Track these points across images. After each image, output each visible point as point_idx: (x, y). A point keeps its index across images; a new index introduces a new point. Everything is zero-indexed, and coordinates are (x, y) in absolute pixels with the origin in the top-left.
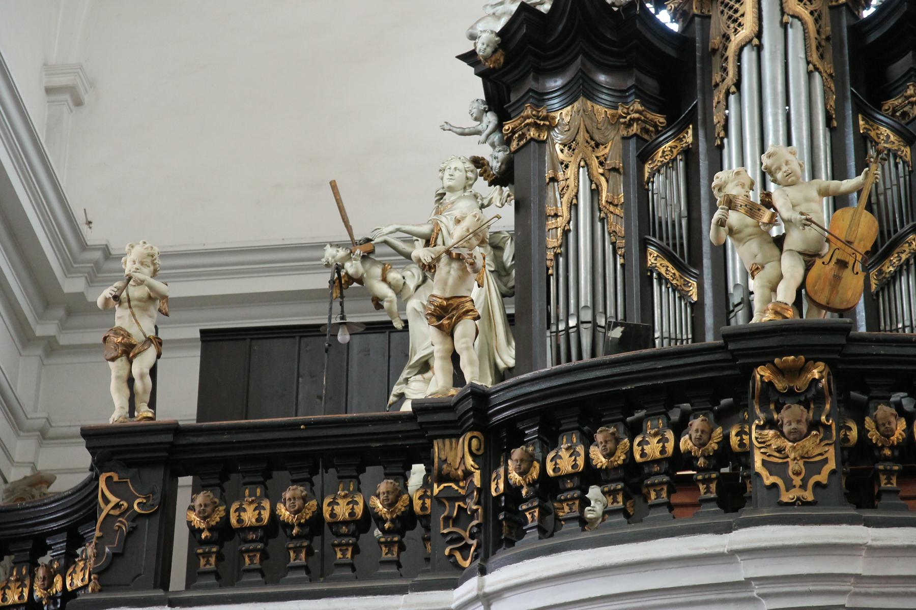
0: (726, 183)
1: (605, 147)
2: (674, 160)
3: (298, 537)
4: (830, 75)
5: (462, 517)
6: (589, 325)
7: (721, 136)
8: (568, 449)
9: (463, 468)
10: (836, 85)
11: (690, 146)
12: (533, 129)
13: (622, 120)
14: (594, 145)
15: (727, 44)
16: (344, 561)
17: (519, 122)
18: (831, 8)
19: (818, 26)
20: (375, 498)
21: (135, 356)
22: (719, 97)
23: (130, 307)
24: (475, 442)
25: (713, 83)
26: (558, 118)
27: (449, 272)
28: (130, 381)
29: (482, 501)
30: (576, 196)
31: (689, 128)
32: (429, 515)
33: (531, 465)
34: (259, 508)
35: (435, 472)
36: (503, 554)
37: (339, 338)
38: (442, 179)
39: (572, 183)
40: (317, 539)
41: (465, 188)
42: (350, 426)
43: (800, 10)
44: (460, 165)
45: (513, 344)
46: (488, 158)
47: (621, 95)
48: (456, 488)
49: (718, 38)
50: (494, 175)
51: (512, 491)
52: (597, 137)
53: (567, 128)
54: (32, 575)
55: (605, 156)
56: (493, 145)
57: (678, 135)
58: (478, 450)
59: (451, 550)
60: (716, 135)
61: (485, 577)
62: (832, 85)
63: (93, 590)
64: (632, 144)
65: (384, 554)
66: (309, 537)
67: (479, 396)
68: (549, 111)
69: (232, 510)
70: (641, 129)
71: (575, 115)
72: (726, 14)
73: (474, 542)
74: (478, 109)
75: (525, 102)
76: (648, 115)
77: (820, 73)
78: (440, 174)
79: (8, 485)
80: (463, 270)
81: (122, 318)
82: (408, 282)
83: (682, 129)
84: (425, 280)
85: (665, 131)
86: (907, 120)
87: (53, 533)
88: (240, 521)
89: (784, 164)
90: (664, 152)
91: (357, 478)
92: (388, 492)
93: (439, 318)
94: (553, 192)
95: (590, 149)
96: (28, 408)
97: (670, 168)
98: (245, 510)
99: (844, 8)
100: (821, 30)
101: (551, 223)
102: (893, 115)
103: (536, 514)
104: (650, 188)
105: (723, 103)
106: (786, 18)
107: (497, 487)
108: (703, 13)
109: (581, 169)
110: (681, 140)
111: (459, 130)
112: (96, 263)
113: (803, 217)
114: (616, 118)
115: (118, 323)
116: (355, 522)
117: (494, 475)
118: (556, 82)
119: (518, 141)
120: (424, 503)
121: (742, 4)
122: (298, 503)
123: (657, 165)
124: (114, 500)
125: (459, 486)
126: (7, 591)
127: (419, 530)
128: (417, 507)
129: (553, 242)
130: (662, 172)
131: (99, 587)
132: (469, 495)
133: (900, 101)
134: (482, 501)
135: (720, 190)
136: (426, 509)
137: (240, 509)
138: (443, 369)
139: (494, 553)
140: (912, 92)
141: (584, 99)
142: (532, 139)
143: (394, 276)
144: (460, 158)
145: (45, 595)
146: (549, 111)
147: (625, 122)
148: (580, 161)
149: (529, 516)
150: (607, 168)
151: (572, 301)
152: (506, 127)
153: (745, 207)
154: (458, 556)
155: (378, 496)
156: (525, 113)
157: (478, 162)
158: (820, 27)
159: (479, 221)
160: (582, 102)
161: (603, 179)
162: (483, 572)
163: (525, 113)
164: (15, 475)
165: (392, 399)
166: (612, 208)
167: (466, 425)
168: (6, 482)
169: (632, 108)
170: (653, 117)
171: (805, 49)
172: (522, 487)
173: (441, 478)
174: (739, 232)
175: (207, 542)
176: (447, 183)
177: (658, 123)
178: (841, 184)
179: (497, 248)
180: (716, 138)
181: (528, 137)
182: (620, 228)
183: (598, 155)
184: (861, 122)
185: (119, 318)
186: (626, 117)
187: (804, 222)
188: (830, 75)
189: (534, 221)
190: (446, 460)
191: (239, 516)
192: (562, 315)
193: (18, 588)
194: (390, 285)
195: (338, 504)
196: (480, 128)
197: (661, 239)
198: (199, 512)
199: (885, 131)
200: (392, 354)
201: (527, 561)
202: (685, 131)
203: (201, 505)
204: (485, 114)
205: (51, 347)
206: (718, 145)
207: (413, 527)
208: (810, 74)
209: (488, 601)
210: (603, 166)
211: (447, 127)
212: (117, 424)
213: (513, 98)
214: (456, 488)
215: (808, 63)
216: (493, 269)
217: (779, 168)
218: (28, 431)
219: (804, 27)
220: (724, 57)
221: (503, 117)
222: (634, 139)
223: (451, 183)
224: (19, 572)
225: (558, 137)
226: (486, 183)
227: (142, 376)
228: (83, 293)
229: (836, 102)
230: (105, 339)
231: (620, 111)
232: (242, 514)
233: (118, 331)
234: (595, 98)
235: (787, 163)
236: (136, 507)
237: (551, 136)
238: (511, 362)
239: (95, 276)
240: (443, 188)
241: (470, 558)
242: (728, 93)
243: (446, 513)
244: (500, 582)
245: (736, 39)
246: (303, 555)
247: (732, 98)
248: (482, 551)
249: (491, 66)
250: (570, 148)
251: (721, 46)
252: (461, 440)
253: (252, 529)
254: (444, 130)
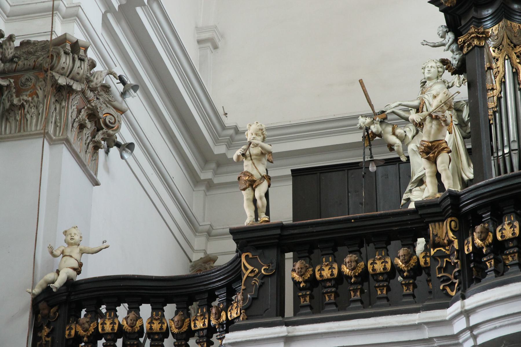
3: (355, 283)
5: (449, 267)
6: (517, 152)
8: (509, 224)
9: (447, 239)
12: (476, 40)
14: (513, 46)
16: (382, 296)
17: (467, 36)
20: (397, 259)
21: (256, 187)
23: (252, 159)
24: (453, 224)
26: (491, 32)
27: (431, 126)
28: (255, 201)
29: (460, 257)
30: (504, 77)
32: (429, 267)
33: (487, 235)
34: (331, 268)
35: (431, 242)
36: (474, 287)
37: (370, 169)
38: (424, 73)
39: (501, 69)
40: (366, 284)
41: (437, 78)
42: (380, 219)
44: (434, 64)
45: (472, 165)
46: (450, 59)
48: (444, 250)
50: (454, 68)
51: (477, 250)
52: (514, 41)
53: (496, 38)
54: (209, 312)
56: (453, 51)
58: (455, 228)
59: (444, 286)
61: (465, 301)
63: (243, 319)
65: (405, 290)
66: (361, 283)
67: (454, 196)
68: (485, 29)
69: (316, 270)
71: (501, 30)
73: (457, 281)
74: (443, 31)
75: (471, 25)
78: (423, 71)
79: (192, 263)
80: (440, 125)
81: (247, 166)
82: (408, 134)
84: (417, 132)
87: (219, 288)
88: (321, 276)
91: (386, 248)
92: (404, 255)
93: (427, 153)
94: (490, 76)
95: (511, 48)
96: (200, 219)
98: (323, 270)
101: (490, 94)
103: (493, 263)
107: (468, 249)
109: (506, 61)
111: (432, 44)
112: (231, 136)
115: (245, 169)
116: (387, 273)
117: (466, 242)
118: (488, 11)
119: (468, 48)
120: (426, 260)
122: (353, 264)
124: (250, 268)
125: (446, 249)
126: (196, 321)
127: (424, 275)
128: (422, 262)
129: (491, 104)
131: (246, 317)
132: (452, 254)
134: (460, 257)
136: (428, 263)
137: (321, 269)
138: (432, 183)
139: (469, 287)
141: (506, 20)
142: (476, 46)
143: (399, 131)
144: (433, 61)
145: (217, 323)
146: (485, 29)
148: (505, 56)
149: (488, 264)
151: (505, 138)
152: (460, 40)
154: (448, 289)
155: (399, 258)
156: (471, 31)
157: (444, 62)
159: (447, 96)
160: (505, 22)
162: (464, 298)
163: (471, 31)
164: (196, 257)
165: (403, 202)
167: (447, 214)
168: (191, 261)
172: (483, 248)
173: (435, 246)
175: (303, 289)
176: (427, 75)
179: (459, 111)
181: (473, 45)
183: (516, 51)
185: (246, 166)
189: (479, 94)
190: (437, 235)
191: (321, 273)
192: (500, 147)
193: (202, 320)
194: (397, 137)
195: (376, 263)
196: (444, 42)
198: (298, 272)
200: (401, 176)
201: (489, 291)
203: (299, 268)
204: (447, 34)
205: (210, 185)
207: (420, 274)
209: (468, 314)
210: (519, 58)
211: (425, 43)
212: (249, 225)
213: (463, 23)
214: (444, 250)
216: (457, 123)
218: (201, 233)
221: (457, 34)
223: (429, 75)
224: (202, 311)
225: (491, 43)
226: (450, 73)
227: (261, 198)
228: (225, 153)
230: (239, 178)
232: (322, 272)
233: (246, 173)
234: (512, 18)
236: (263, 271)
237: (487, 43)
238: (472, 176)
239: (231, 144)
240: (425, 78)
241: (455, 290)
243: (439, 265)
244: (474, 303)
246: (358, 293)
248: (462, 286)
249: (449, 5)
250: (499, 49)
252: (445, 223)
253: (328, 280)
254: (423, 45)
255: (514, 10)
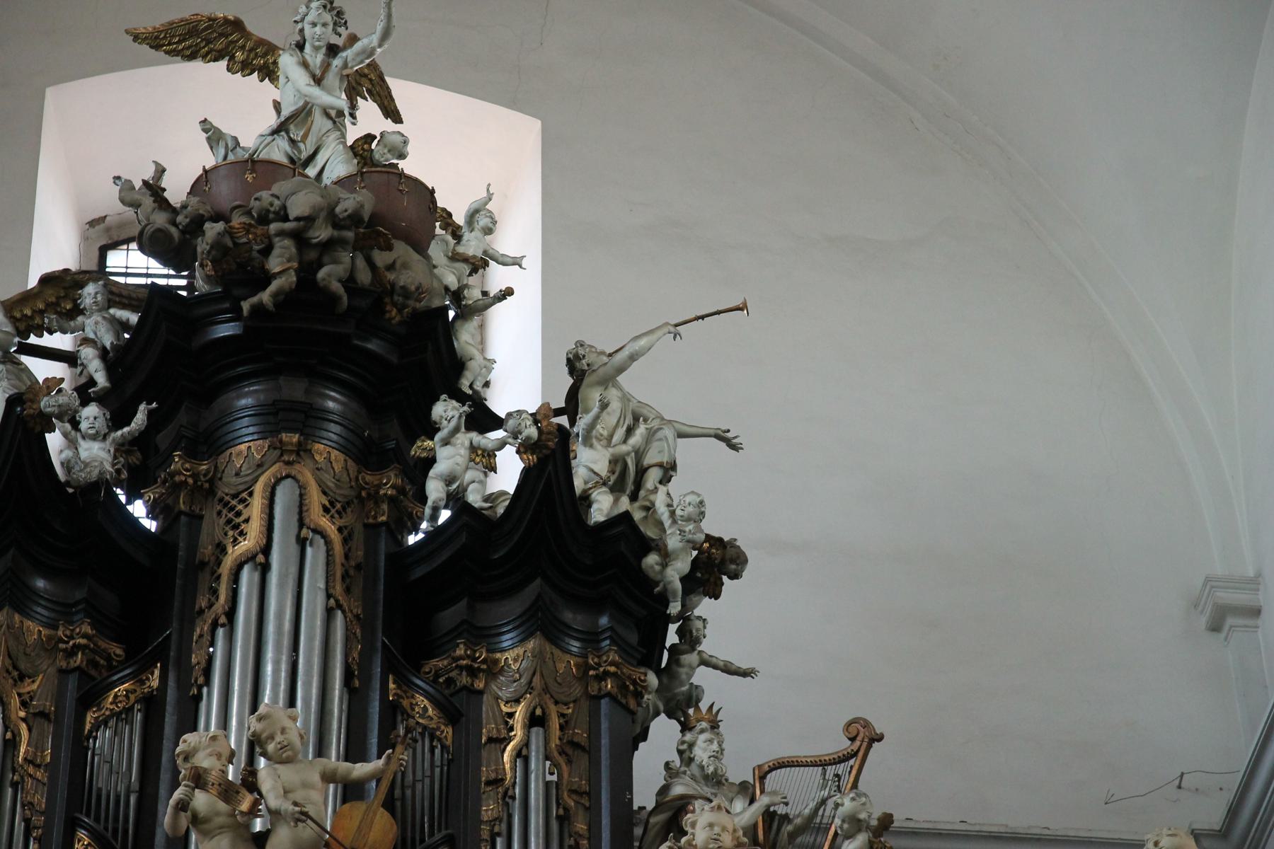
0: (195, 751)
1: (33, 682)
2: (129, 710)
4: (357, 617)
7: (199, 683)
10: (362, 628)
11: (155, 693)
13: (62, 646)
14: (17, 677)
15: (221, 557)
18: (366, 526)
19: (347, 547)
22: (202, 629)
25: (197, 607)
31: (156, 667)
43: (325, 523)
47: (63, 612)
49: (210, 547)
52: (22, 666)
55: (32, 694)
57: (139, 676)
60: (193, 681)
62: (358, 630)
64: (72, 682)
70: (87, 661)
72: (224, 516)
76: (100, 643)
77: (344, 612)
83: (147, 667)
85: (121, 668)
86: (452, 689)
89: (279, 733)
90: (116, 696)
95: (10, 681)
97: (122, 720)
99: (384, 528)
100: (350, 554)
102: (435, 681)
104: (91, 745)
105: (207, 638)
106: (304, 531)
108: (193, 511)
110: (142, 682)
113: (297, 809)
114: (53, 642)
121: (247, 506)
123: (104, 714)
130: (110, 724)
133: (445, 662)
135: (186, 759)
140: (462, 652)
147: (67, 648)
150: (32, 711)
153: (218, 787)
158: (350, 549)
160: (7, 614)
161: (23, 727)
166: (31, 770)
169: (78, 630)
170: (107, 646)
171: (327, 577)
174: (206, 820)
177: (112, 655)
178: (354, 767)
180: (193, 685)
182: (40, 800)
184: (392, 686)
186: (68, 642)
187: (297, 816)
188: (357, 617)
197: (97, 820)
199: (421, 701)
202: (150, 670)
206: (193, 694)
208: (329, 612)
210: (25, 707)
215: (329, 596)
217: (272, 737)
219: (327, 547)
220: (216, 575)
222: (77, 674)
229: (360, 654)
231: (60, 633)
234: (28, 610)
235: (283, 731)
242: (215, 625)
245: (236, 551)
247: (220, 632)
251: (213, 559)
255: (35, 592)
